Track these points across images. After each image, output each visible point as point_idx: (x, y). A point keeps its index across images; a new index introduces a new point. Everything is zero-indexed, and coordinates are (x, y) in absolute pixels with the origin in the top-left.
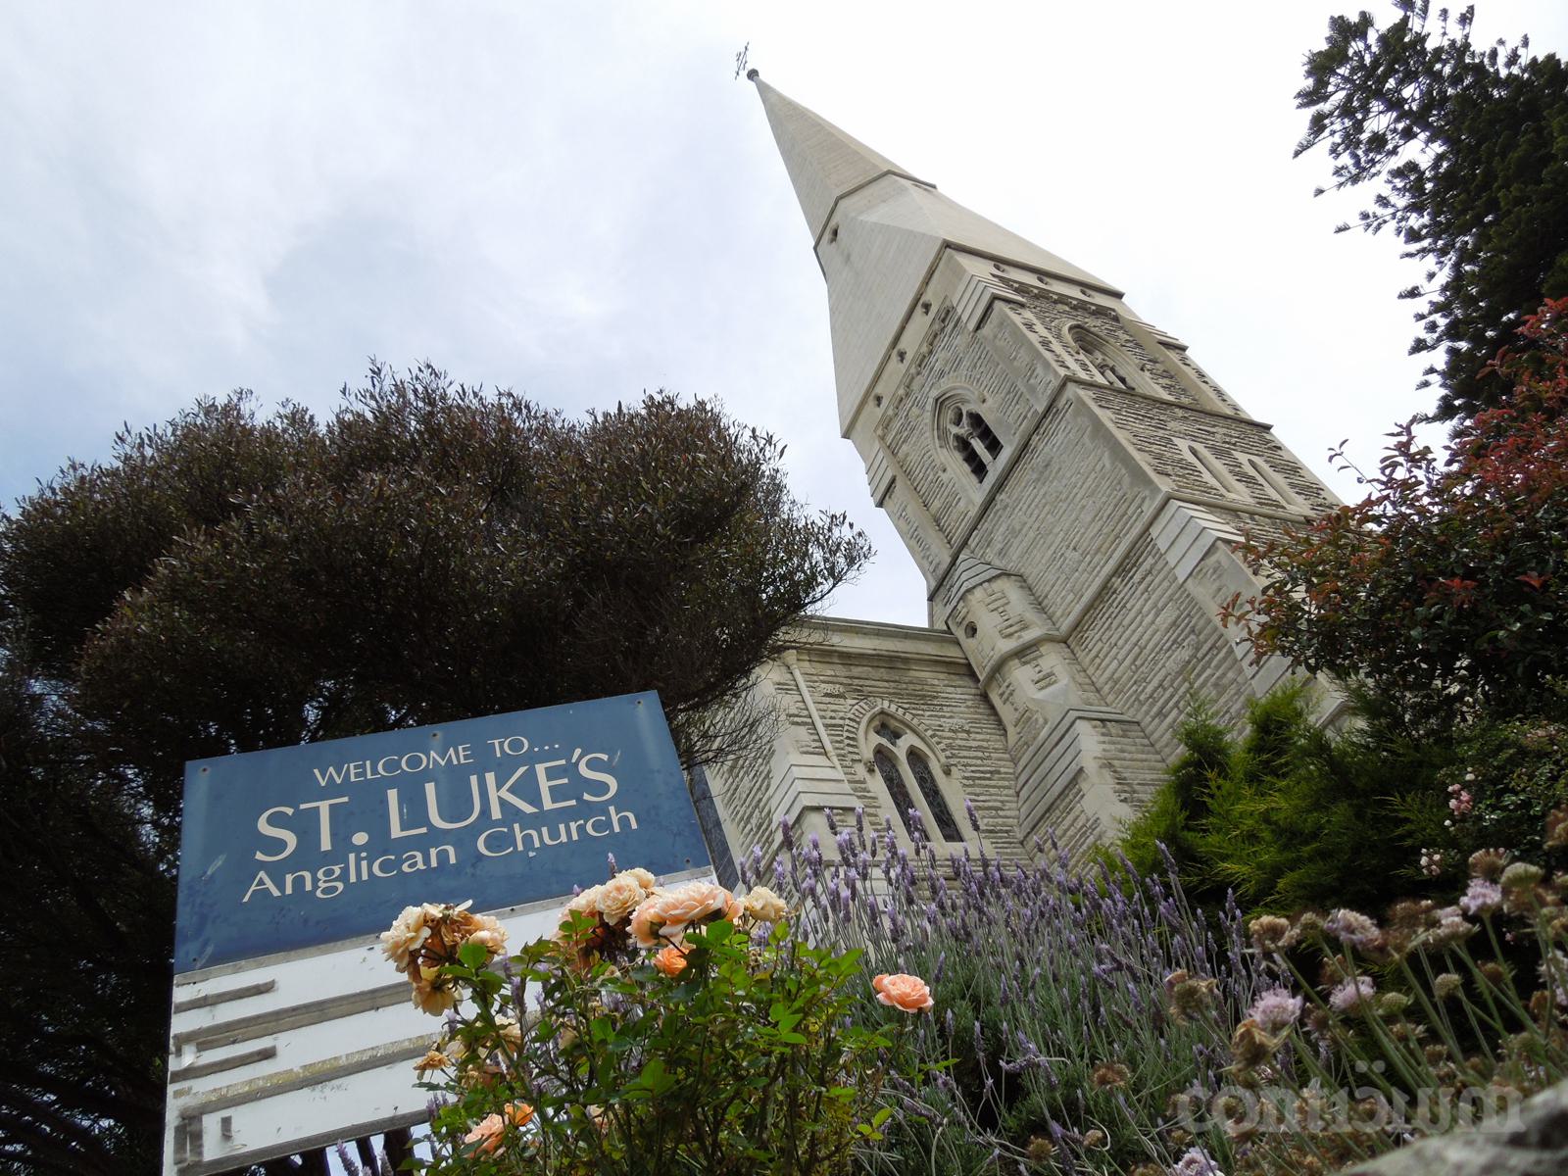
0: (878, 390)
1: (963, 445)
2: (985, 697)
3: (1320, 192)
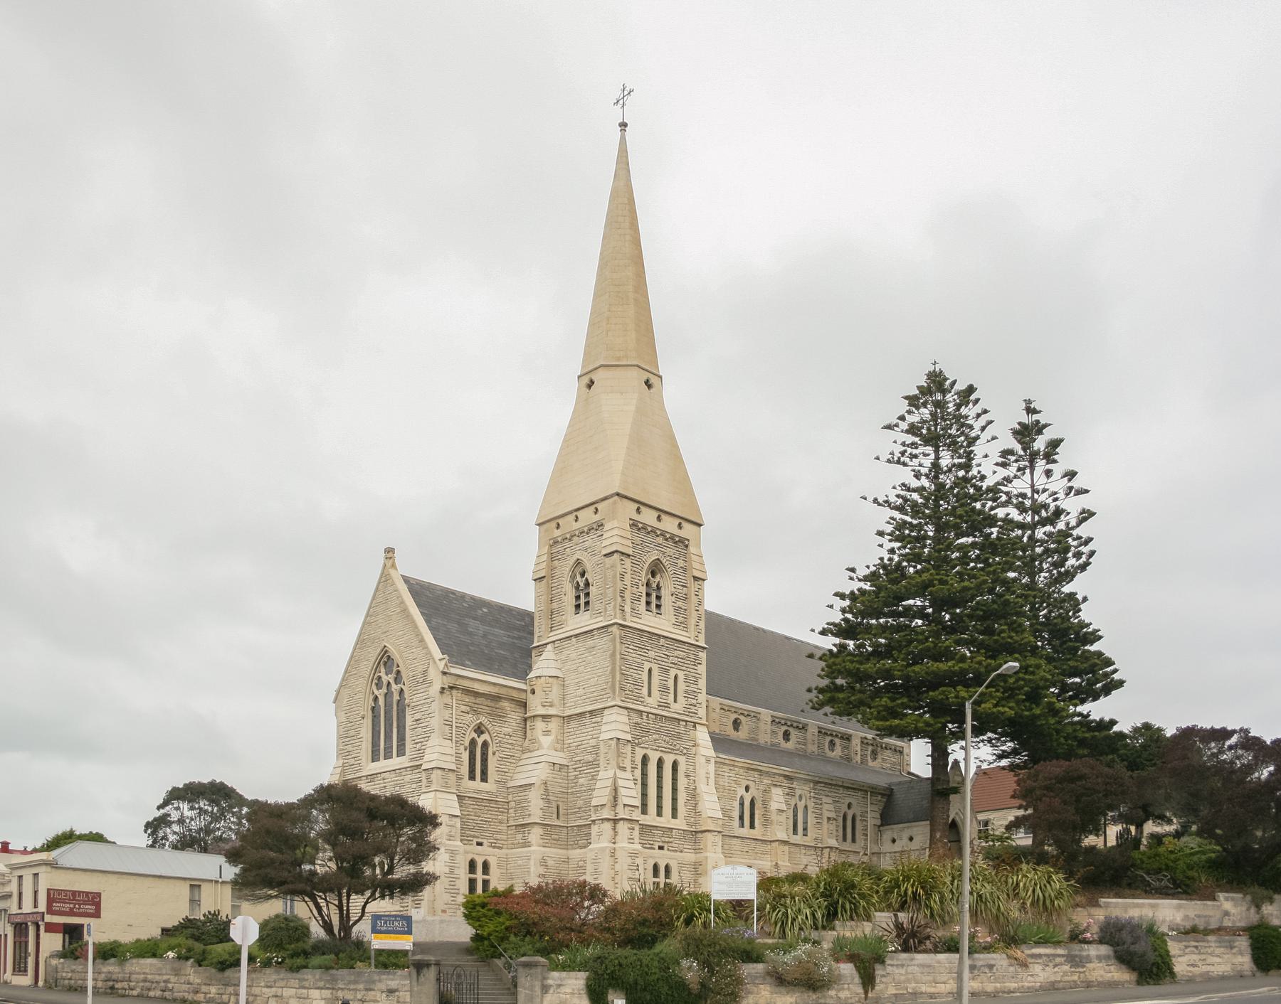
0: (560, 521)
2: (525, 720)
3: (878, 458)
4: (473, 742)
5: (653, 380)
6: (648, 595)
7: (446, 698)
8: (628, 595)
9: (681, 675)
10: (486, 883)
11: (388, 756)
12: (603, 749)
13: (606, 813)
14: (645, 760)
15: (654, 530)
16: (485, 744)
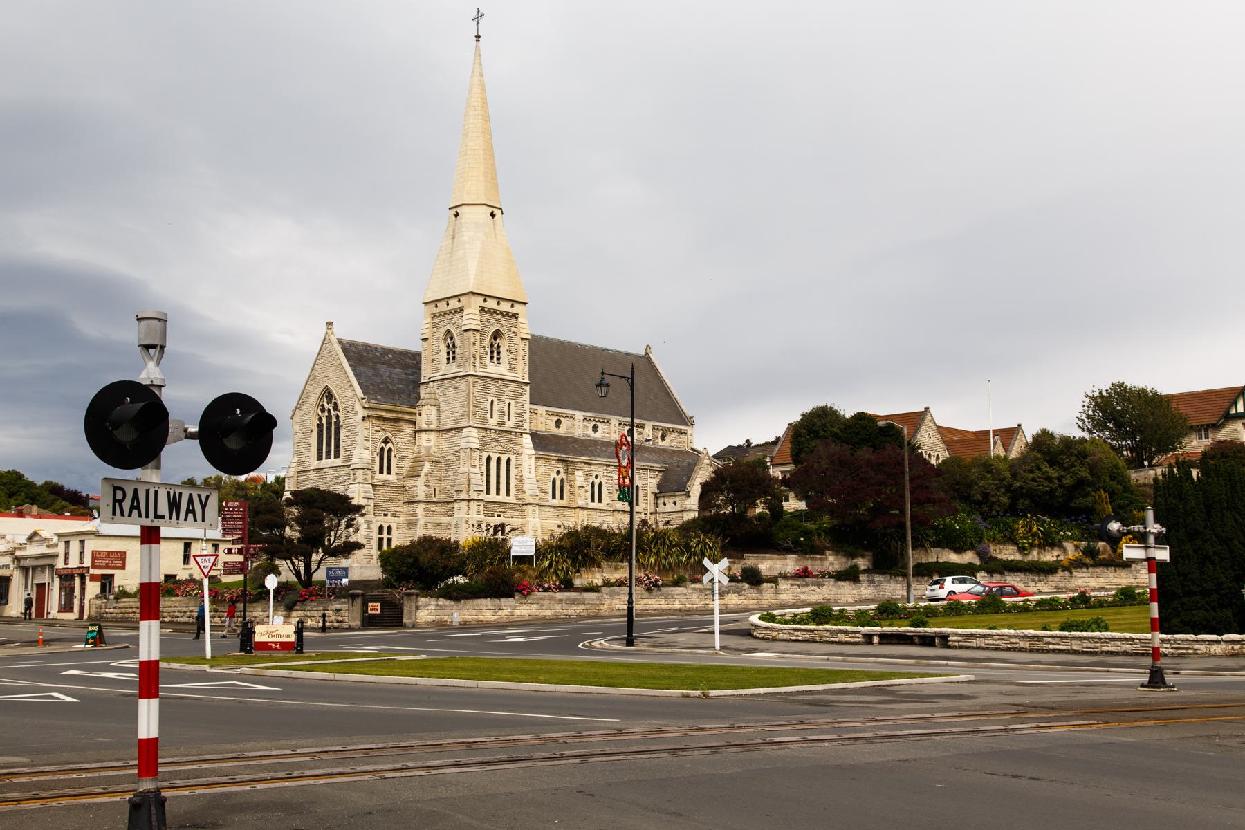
4: (382, 449)
5: (497, 212)
6: (492, 352)
7: (366, 424)
8: (478, 355)
9: (513, 402)
10: (389, 540)
11: (328, 457)
12: (462, 454)
13: (464, 496)
14: (489, 459)
15: (495, 311)
16: (390, 450)
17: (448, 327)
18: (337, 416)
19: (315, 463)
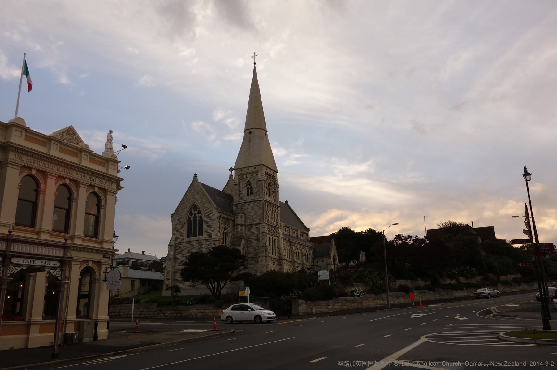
1: (248, 188)
11: (195, 235)
13: (264, 254)
17: (249, 179)
18: (201, 217)
19: (187, 239)
